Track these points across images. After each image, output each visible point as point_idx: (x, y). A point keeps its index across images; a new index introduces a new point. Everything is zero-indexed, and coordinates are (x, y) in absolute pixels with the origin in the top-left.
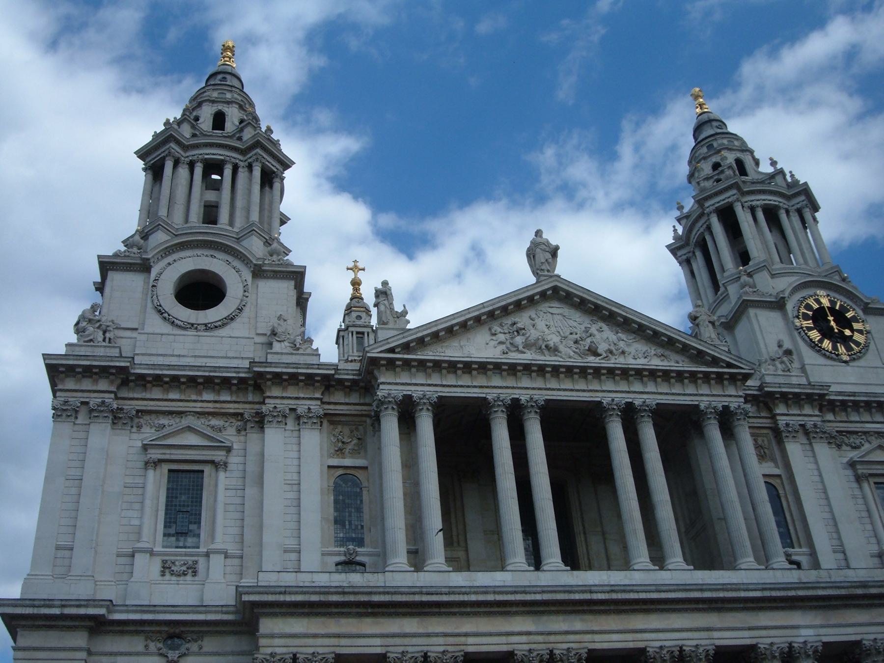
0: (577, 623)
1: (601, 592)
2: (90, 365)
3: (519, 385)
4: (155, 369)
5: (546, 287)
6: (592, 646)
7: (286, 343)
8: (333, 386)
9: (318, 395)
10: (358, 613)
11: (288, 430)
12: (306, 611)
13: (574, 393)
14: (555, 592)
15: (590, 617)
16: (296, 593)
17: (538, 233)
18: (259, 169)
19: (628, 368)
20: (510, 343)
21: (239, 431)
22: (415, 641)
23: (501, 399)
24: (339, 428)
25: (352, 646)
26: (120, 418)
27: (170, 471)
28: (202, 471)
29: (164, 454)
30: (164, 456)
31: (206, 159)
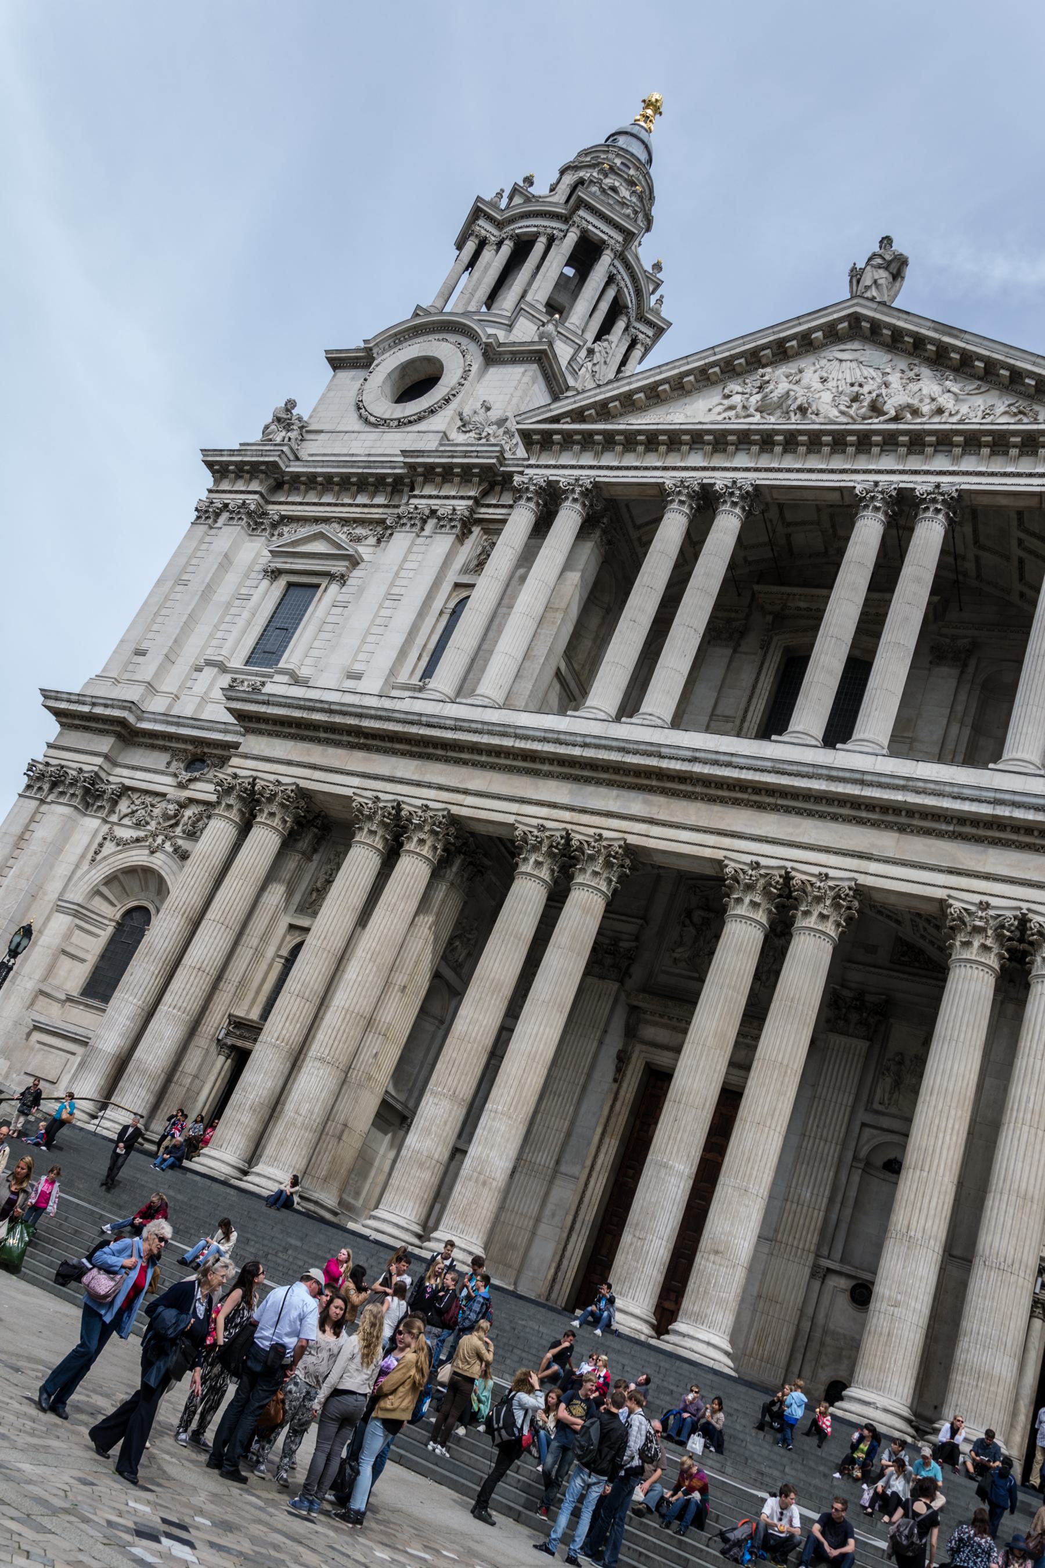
0: (636, 804)
1: (677, 759)
2: (241, 461)
4: (309, 467)
5: (835, 316)
6: (632, 840)
7: (472, 434)
9: (472, 493)
10: (349, 742)
12: (293, 731)
13: (813, 476)
15: (661, 800)
17: (886, 241)
19: (924, 430)
20: (744, 407)
21: (379, 541)
23: (686, 484)
26: (262, 523)
31: (517, 235)
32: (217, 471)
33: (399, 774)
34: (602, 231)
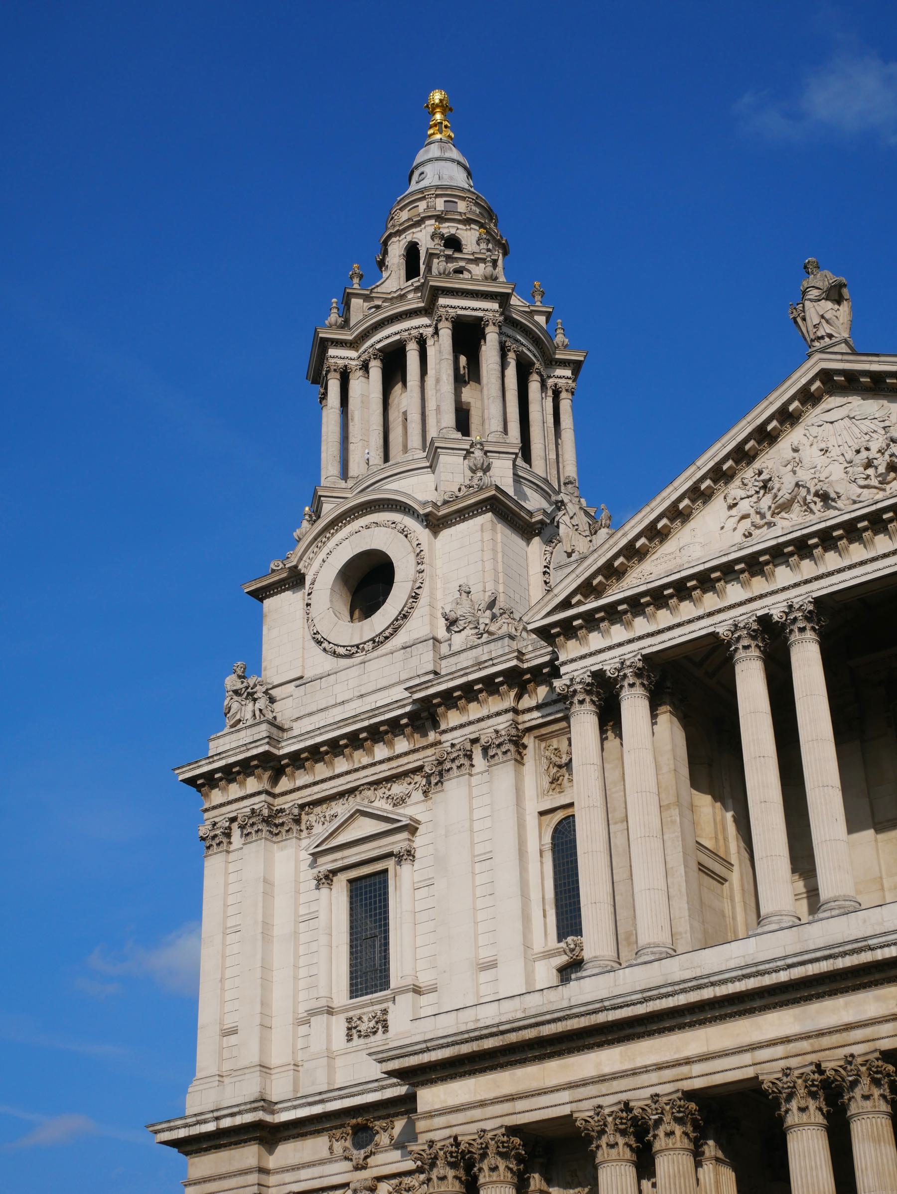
1: (888, 946)
3: (773, 587)
5: (804, 381)
8: (529, 681)
11: (478, 774)
14: (811, 961)
16: (442, 1047)
18: (449, 332)
22: (616, 1085)
24: (555, 743)
25: (532, 1110)
26: (282, 824)
27: (351, 881)
28: (386, 871)
29: (336, 860)
30: (335, 864)
31: (380, 350)
32: (203, 785)
33: (607, 1070)
34: (473, 309)
